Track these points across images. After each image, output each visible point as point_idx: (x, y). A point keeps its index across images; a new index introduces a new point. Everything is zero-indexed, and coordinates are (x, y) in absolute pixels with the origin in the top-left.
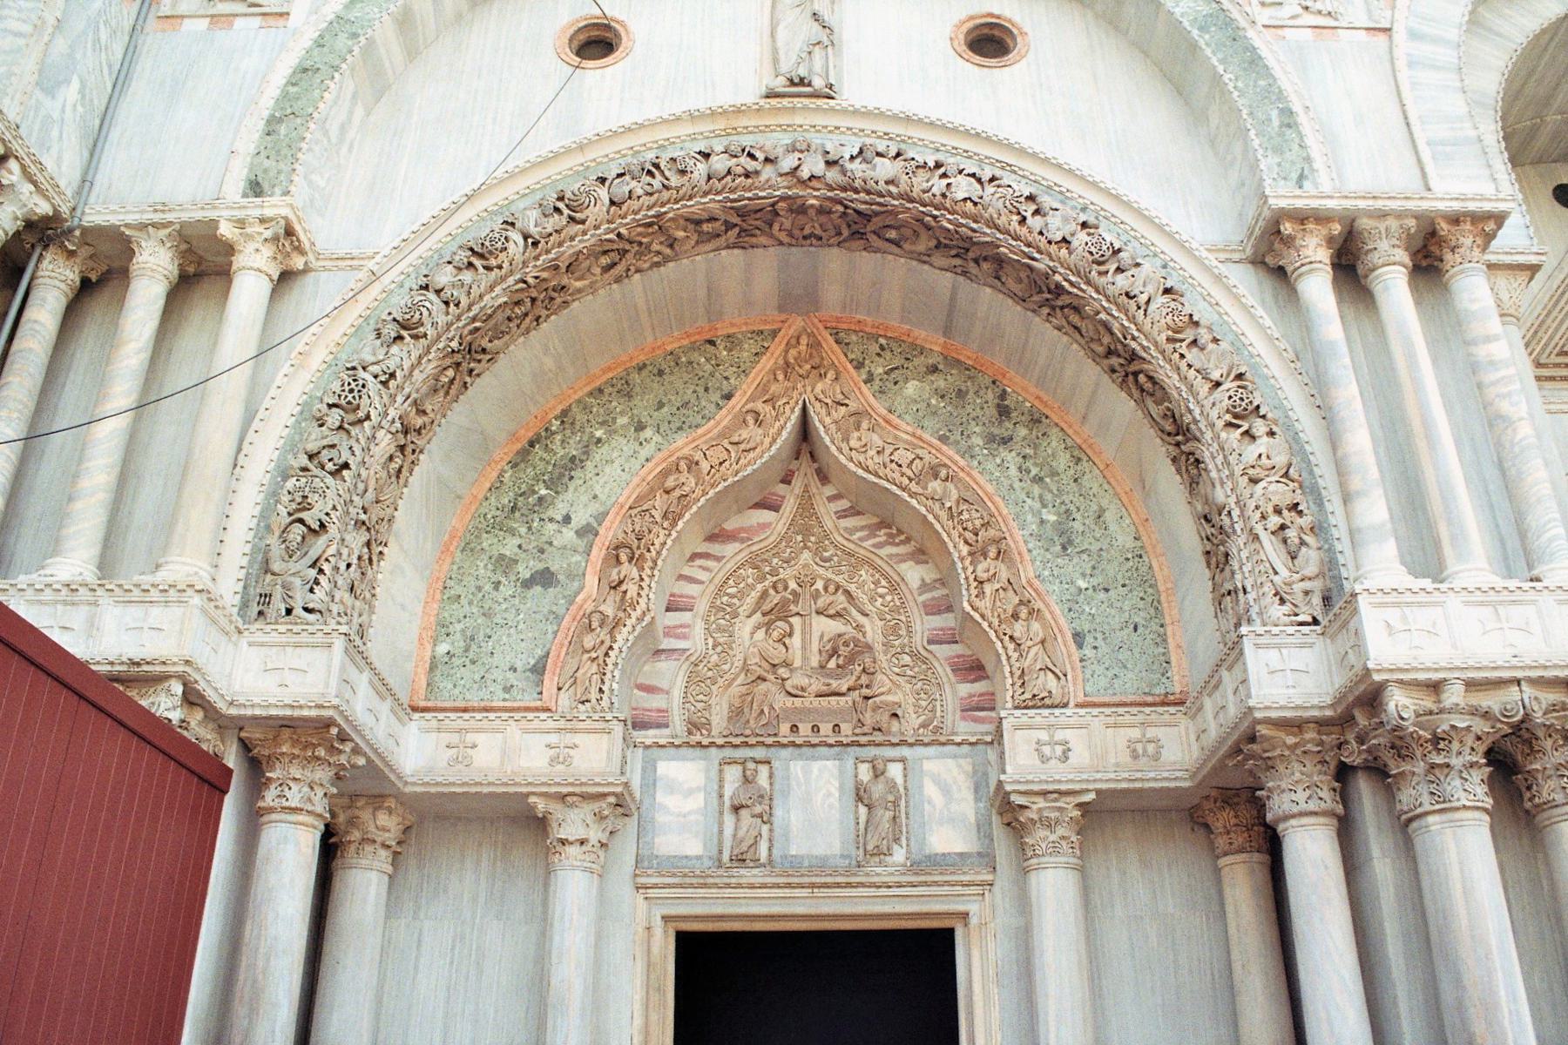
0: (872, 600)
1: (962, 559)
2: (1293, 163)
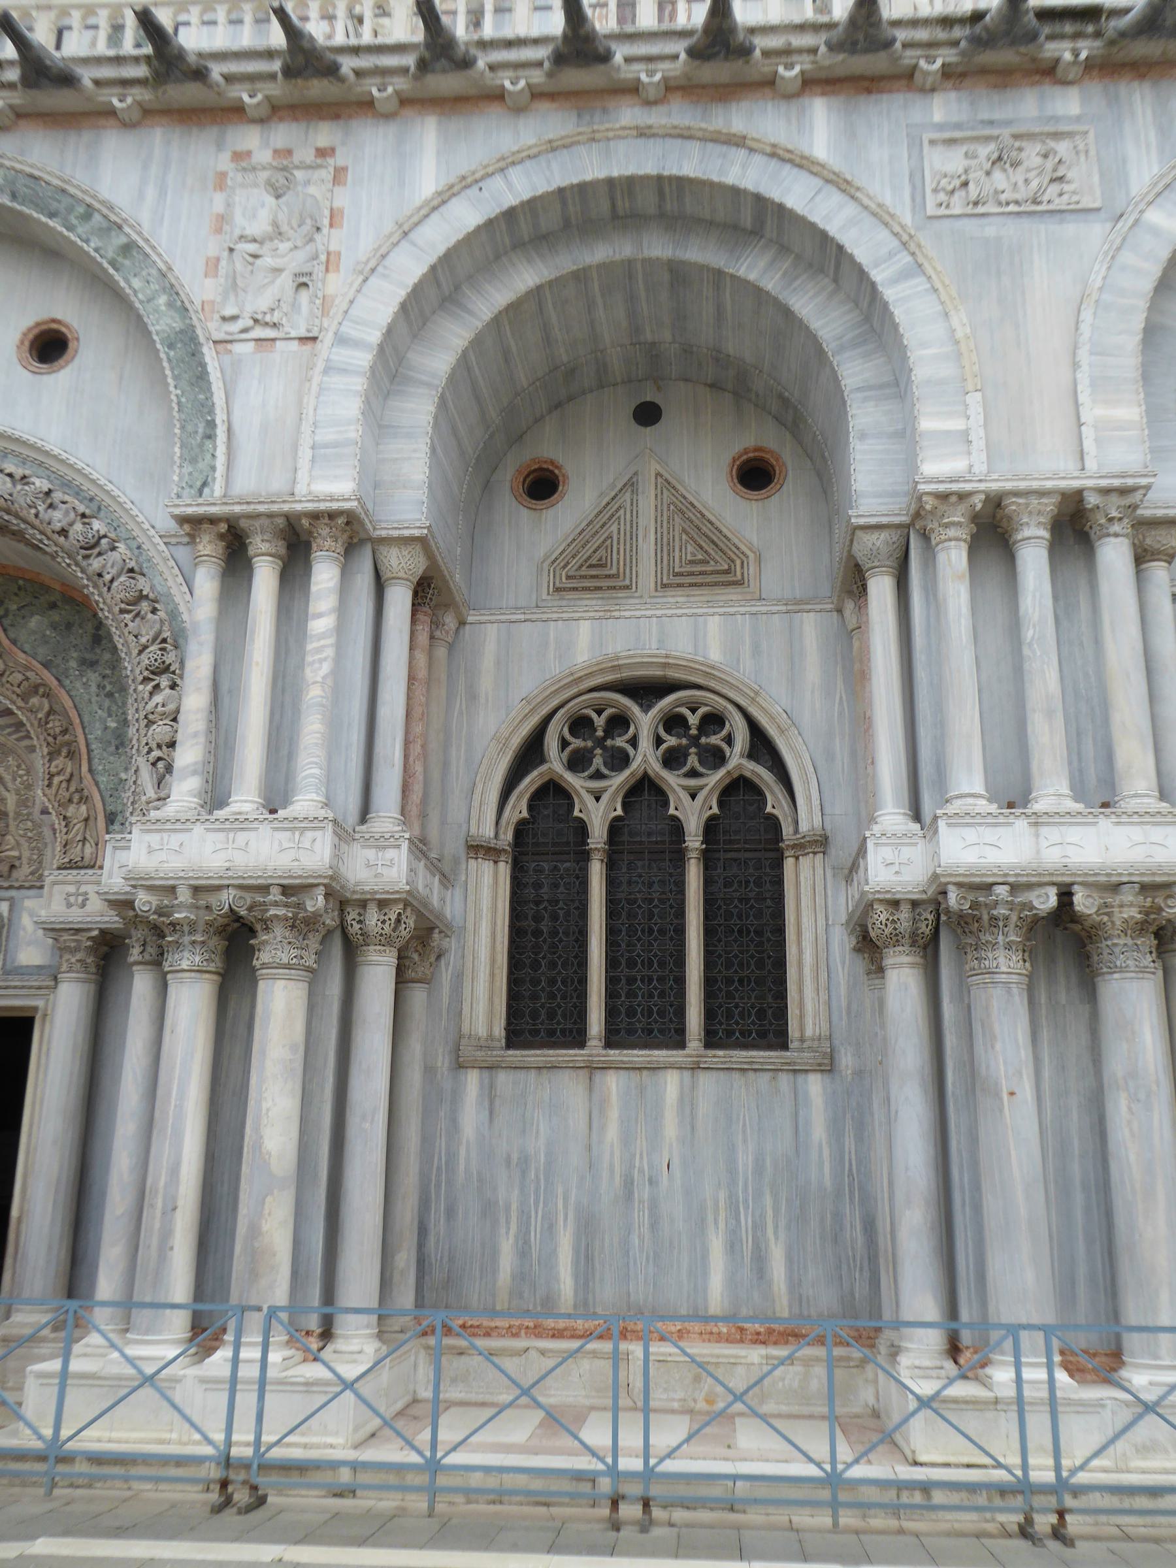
0: (14, 779)
1: (43, 757)
2: (201, 472)
